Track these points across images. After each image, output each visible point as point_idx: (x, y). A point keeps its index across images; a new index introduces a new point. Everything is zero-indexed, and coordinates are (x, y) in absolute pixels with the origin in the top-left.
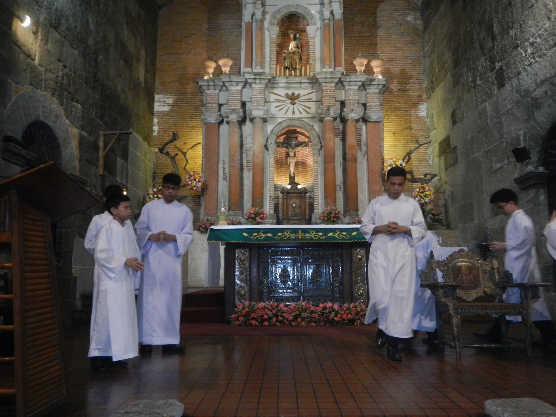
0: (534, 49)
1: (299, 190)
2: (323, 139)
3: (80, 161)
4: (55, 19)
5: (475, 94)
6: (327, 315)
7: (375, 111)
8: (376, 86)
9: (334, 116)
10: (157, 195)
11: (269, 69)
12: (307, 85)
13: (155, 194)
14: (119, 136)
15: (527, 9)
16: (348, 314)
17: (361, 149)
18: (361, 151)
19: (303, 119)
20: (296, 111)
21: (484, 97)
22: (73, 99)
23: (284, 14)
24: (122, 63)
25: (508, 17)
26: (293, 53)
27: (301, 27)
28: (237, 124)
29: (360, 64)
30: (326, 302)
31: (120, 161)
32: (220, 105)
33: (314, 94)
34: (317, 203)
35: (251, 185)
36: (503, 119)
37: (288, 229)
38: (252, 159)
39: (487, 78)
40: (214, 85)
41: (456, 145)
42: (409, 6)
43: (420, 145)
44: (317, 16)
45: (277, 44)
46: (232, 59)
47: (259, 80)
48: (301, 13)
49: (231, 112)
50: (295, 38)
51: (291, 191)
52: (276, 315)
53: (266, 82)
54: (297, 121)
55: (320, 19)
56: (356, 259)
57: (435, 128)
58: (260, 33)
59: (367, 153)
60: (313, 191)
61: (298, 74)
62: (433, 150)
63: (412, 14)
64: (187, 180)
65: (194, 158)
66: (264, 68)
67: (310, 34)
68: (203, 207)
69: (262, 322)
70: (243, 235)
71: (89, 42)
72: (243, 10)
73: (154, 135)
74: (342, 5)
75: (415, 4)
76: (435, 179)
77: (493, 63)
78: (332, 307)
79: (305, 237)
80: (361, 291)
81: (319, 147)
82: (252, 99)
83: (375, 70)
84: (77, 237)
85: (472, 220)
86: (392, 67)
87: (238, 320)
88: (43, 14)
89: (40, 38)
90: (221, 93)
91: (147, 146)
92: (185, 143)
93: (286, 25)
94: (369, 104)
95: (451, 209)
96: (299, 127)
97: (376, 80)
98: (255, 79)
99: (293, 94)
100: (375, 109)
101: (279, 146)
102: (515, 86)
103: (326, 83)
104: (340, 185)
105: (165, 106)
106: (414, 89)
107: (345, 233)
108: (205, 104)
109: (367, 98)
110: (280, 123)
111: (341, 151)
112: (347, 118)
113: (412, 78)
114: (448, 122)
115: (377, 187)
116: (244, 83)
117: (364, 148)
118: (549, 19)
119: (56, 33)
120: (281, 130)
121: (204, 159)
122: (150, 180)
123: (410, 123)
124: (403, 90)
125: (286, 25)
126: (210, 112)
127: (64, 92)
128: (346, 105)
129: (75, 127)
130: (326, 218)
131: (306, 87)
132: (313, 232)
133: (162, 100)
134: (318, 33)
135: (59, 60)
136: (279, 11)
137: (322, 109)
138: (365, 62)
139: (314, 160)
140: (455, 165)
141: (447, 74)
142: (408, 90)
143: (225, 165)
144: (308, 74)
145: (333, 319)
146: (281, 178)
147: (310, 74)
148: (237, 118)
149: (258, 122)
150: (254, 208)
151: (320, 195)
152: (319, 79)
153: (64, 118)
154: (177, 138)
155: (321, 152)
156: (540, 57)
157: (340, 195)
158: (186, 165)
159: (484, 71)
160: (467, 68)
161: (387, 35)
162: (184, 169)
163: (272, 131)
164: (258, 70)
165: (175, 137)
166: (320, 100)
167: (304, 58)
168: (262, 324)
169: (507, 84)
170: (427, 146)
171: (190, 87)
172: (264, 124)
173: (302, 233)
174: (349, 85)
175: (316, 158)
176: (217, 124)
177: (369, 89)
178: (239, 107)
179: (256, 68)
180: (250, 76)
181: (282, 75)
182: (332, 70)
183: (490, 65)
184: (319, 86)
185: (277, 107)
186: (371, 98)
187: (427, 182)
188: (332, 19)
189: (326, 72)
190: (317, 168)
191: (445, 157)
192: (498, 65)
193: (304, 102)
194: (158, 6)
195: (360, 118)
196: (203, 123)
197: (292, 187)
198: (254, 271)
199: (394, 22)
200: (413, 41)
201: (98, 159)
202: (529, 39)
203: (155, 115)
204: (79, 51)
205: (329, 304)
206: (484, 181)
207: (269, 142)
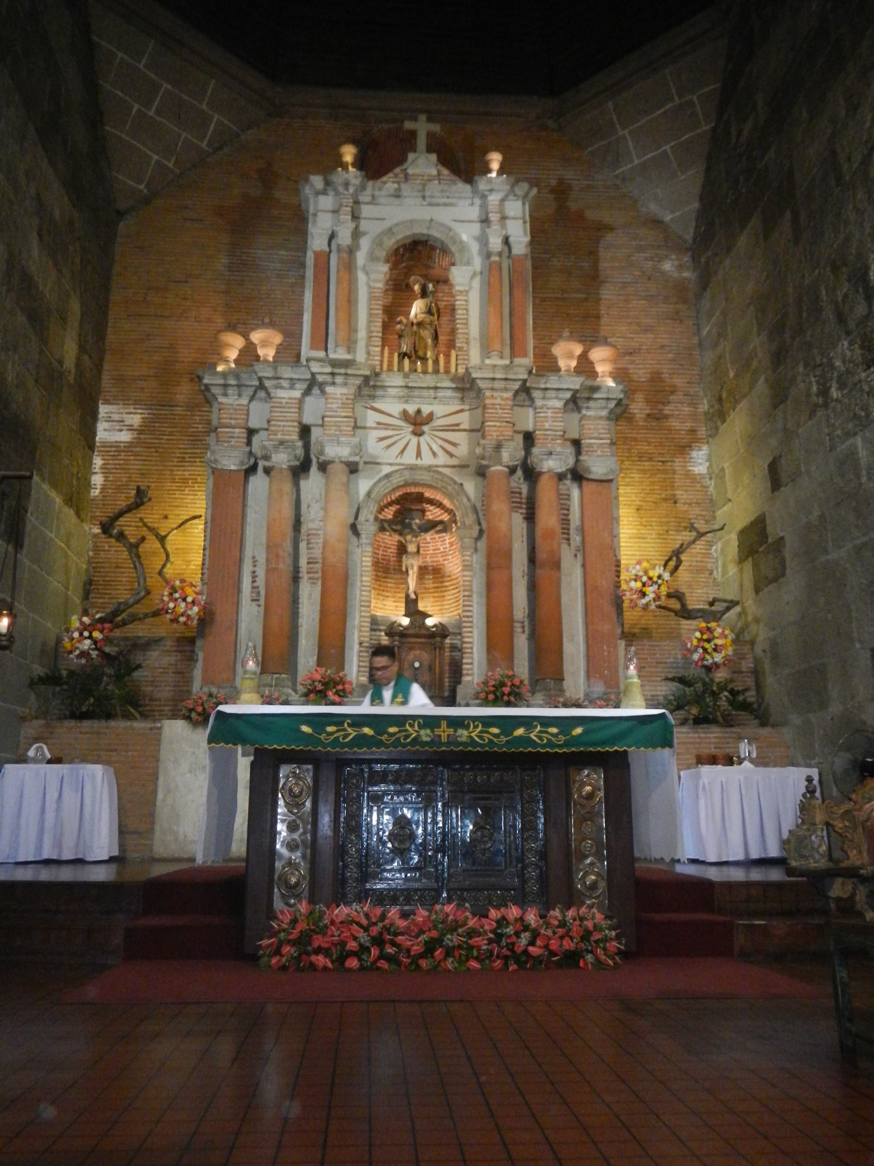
1: (428, 628)
2: (484, 515)
5: (828, 420)
6: (509, 941)
7: (599, 456)
9: (511, 464)
10: (91, 633)
12: (449, 393)
13: (85, 629)
16: (562, 938)
17: (568, 539)
18: (569, 545)
19: (440, 469)
20: (425, 450)
21: (850, 426)
24: (21, 319)
26: (420, 324)
27: (436, 272)
28: (287, 475)
30: (506, 906)
33: (466, 414)
34: (470, 661)
35: (317, 616)
38: (320, 556)
39: (855, 385)
41: (781, 534)
43: (701, 535)
44: (475, 247)
45: (384, 306)
48: (436, 240)
49: (276, 447)
50: (424, 293)
51: (411, 632)
52: (378, 941)
53: (358, 381)
54: (427, 473)
55: (480, 253)
56: (580, 796)
57: (730, 500)
59: (583, 548)
60: (460, 634)
61: (430, 369)
62: (722, 549)
63: (674, 257)
64: (166, 599)
66: (355, 352)
67: (459, 285)
68: (200, 664)
72: (310, 225)
73: (92, 494)
74: (528, 225)
75: (680, 237)
78: (521, 919)
79: (459, 736)
80: (593, 877)
81: (475, 533)
83: (600, 368)
85: (823, 705)
86: (632, 366)
87: (277, 952)
90: (254, 406)
91: (74, 519)
92: (166, 517)
93: (404, 264)
94: (588, 441)
95: (770, 681)
97: (602, 390)
98: (333, 374)
99: (419, 412)
100: (599, 453)
101: (382, 529)
103: (492, 389)
105: (121, 430)
107: (554, 730)
108: (216, 429)
109: (582, 427)
110: (387, 476)
111: (525, 543)
112: (538, 469)
114: (762, 484)
115: (606, 627)
116: (307, 383)
117: (576, 539)
120: (390, 493)
121: (207, 553)
122: (77, 600)
123: (673, 488)
124: (657, 417)
125: (404, 264)
126: (226, 445)
128: (536, 441)
130: (491, 697)
131: (449, 398)
132: (477, 726)
133: (116, 417)
134: (476, 283)
138: (578, 349)
139: (464, 561)
140: (781, 580)
141: (757, 382)
142: (666, 417)
143: (256, 569)
144: (453, 370)
145: (525, 952)
146: (385, 602)
147: (456, 370)
148: (289, 461)
149: (338, 473)
150: (323, 669)
151: (475, 642)
152: (478, 381)
154: (145, 500)
155: (479, 544)
157: (522, 643)
158: (164, 566)
159: (847, 369)
160: (806, 365)
161: (622, 298)
162: (160, 573)
163: (369, 494)
164: (340, 354)
165: (141, 499)
166: (478, 427)
167: (442, 338)
168: (342, 963)
170: (710, 539)
171: (184, 392)
172: (353, 476)
173: (449, 726)
174: (544, 398)
175: (468, 558)
176: (243, 473)
177: (587, 408)
178: (295, 437)
179: (335, 352)
180: (322, 367)
181: (396, 368)
182: (507, 362)
183: (863, 355)
184: (478, 397)
185: (382, 439)
186: (590, 429)
187: (716, 617)
188: (506, 254)
189: (495, 366)
190: (471, 581)
191: (755, 566)
193: (442, 430)
194: (118, 212)
195: (567, 470)
196: (210, 471)
197: (411, 622)
198: (326, 820)
199: (636, 273)
200: (677, 313)
203: (96, 449)
205: (514, 912)
206: (854, 614)
207: (361, 518)
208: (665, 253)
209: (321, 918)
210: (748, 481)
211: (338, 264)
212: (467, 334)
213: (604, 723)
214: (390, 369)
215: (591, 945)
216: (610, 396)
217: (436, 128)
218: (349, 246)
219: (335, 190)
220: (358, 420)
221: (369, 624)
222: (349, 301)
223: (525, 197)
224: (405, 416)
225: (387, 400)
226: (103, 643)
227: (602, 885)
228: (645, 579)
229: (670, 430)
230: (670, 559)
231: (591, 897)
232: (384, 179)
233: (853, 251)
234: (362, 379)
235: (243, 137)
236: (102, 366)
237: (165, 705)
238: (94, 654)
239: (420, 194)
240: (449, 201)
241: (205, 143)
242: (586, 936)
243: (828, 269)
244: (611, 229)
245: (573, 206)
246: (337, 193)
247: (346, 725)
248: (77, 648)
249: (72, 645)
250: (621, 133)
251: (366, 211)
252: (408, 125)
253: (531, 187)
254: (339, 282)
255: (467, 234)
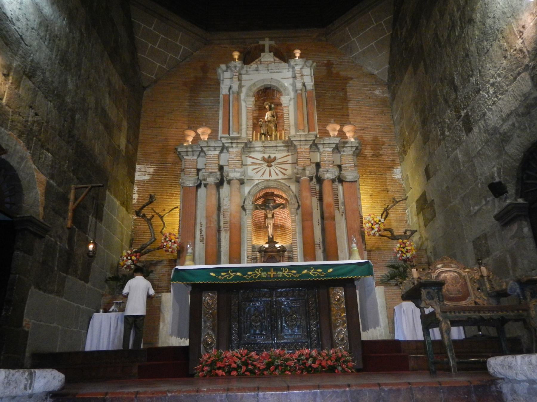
0: (495, 89)
1: (276, 248)
3: (45, 208)
4: (30, 69)
5: (445, 145)
6: (304, 362)
8: (350, 148)
9: (310, 176)
10: (131, 257)
11: (246, 135)
12: (282, 148)
13: (129, 256)
14: (90, 190)
15: (484, 55)
16: (327, 360)
17: (338, 208)
21: (454, 146)
22: (42, 146)
23: (260, 87)
24: (101, 127)
25: (467, 67)
26: (269, 121)
28: (214, 187)
29: (333, 129)
31: (92, 219)
32: (198, 170)
33: (291, 156)
36: (475, 161)
37: (259, 267)
39: (454, 128)
40: (193, 151)
41: (433, 199)
42: (376, 82)
44: (291, 88)
46: (210, 127)
47: (236, 144)
48: (274, 86)
50: (270, 109)
52: (246, 364)
53: (242, 145)
55: (293, 90)
57: (411, 188)
58: (236, 103)
59: (345, 212)
60: (292, 251)
62: (410, 210)
65: (173, 224)
69: (229, 372)
70: (210, 275)
71: (66, 98)
72: (221, 85)
74: (313, 78)
75: (382, 80)
76: (416, 237)
77: (459, 112)
78: (310, 354)
79: (278, 275)
81: (296, 206)
82: (229, 162)
83: (348, 135)
84: (33, 287)
86: (364, 135)
88: (17, 61)
89: (10, 81)
91: (125, 212)
96: (276, 188)
98: (232, 143)
99: (269, 157)
100: (350, 170)
101: (257, 208)
102: (482, 127)
103: (300, 145)
104: (319, 243)
105: (145, 175)
106: (387, 154)
107: (320, 270)
108: (184, 169)
109: (341, 159)
110: (257, 184)
111: (319, 211)
112: (323, 178)
113: (384, 144)
116: (221, 148)
117: (342, 208)
118: (505, 57)
119: (30, 82)
121: (181, 222)
127: (33, 138)
129: (42, 173)
132: (286, 270)
133: (143, 170)
134: (292, 103)
135: (31, 107)
136: (254, 84)
137: (298, 169)
138: (338, 127)
139: (292, 219)
140: (434, 219)
142: (381, 155)
144: (283, 138)
145: (310, 366)
148: (214, 181)
149: (236, 184)
151: (299, 254)
152: (294, 142)
153: (31, 162)
155: (298, 211)
156: (502, 94)
158: (163, 229)
160: (435, 124)
162: (161, 232)
163: (249, 193)
164: (235, 135)
168: (230, 374)
169: (474, 128)
171: (171, 158)
172: (242, 186)
173: (274, 270)
174: (323, 148)
176: (195, 187)
177: (343, 151)
178: (217, 170)
180: (227, 140)
182: (306, 133)
183: (456, 115)
184: (295, 149)
185: (254, 169)
186: (345, 160)
188: (304, 90)
189: (300, 135)
190: (295, 227)
191: (424, 215)
192: (463, 113)
194: (143, 87)
195: (336, 177)
201: (66, 212)
202: (489, 80)
204: (54, 104)
205: (306, 351)
207: (246, 203)
208: (376, 87)
209: (220, 355)
210: (417, 178)
211: (233, 99)
212: (289, 123)
213: (341, 266)
214: (256, 139)
215: (340, 363)
216: (353, 145)
217: (273, 43)
218: (237, 91)
219: (231, 70)
220: (243, 162)
221: (251, 249)
222: (238, 113)
223: (311, 66)
224: (264, 159)
225: (255, 153)
226: (136, 261)
227: (346, 339)
228: (372, 222)
229: (383, 160)
230: (383, 213)
231: (341, 345)
232: (252, 64)
233: (448, 73)
234: (244, 144)
235: (195, 54)
236: (137, 149)
237: (164, 290)
238: (133, 266)
239: (267, 69)
240: (279, 70)
241: (179, 57)
242: (338, 359)
243: (439, 82)
244: (352, 79)
245: (334, 71)
246: (232, 71)
247: (229, 272)
248: (126, 264)
249: (123, 263)
250: (353, 39)
251: (244, 77)
252: (261, 42)
253: (314, 62)
254: (233, 106)
255: (287, 83)
